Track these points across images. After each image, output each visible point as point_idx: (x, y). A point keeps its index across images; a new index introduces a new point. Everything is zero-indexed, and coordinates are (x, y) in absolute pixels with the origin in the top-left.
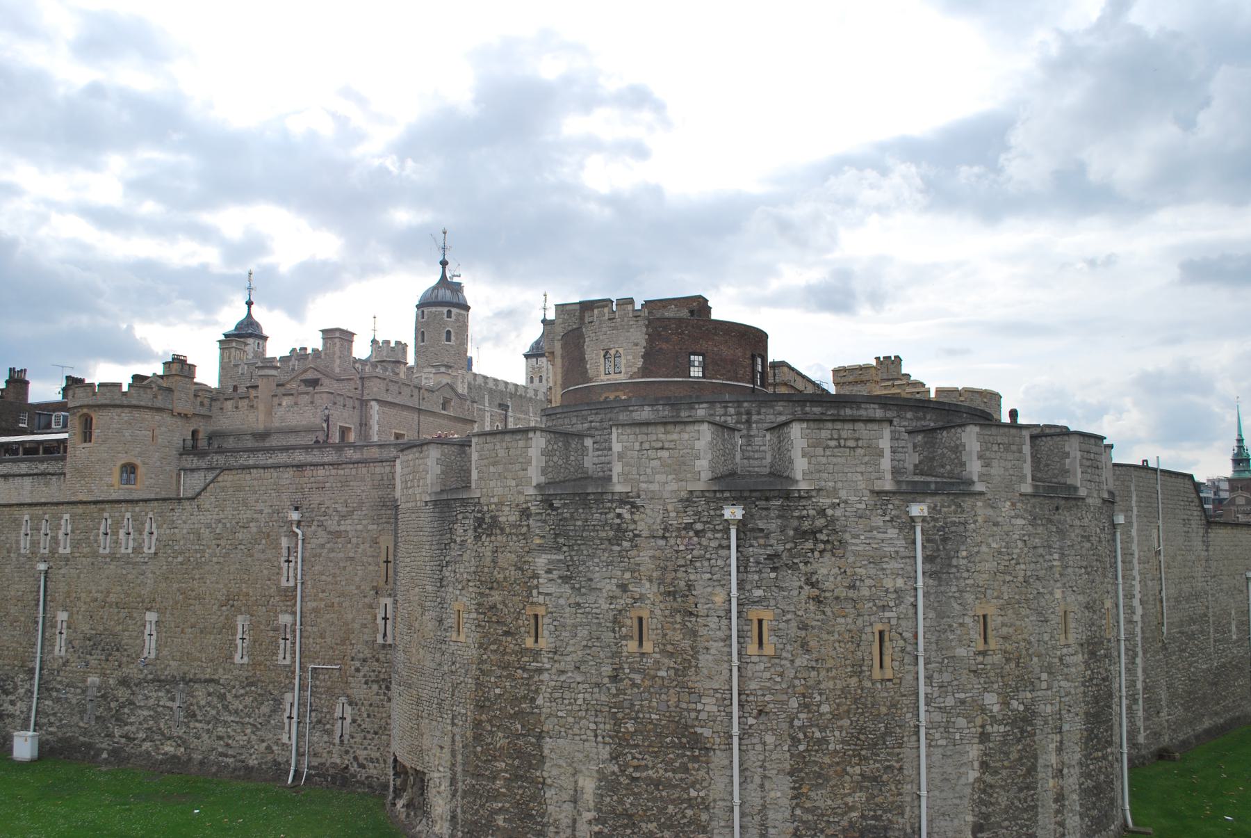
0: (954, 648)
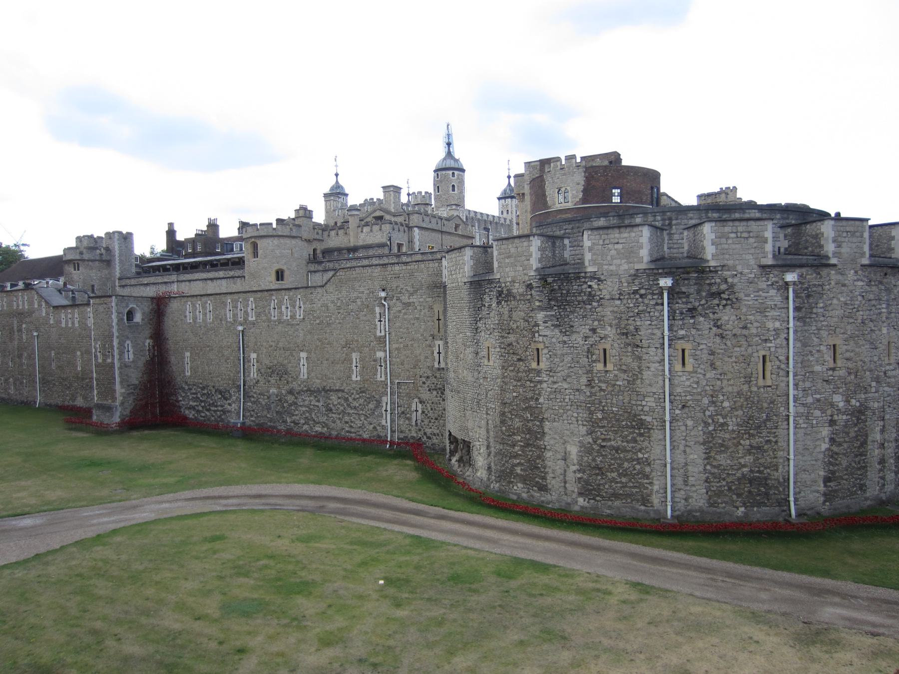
0: (813, 366)
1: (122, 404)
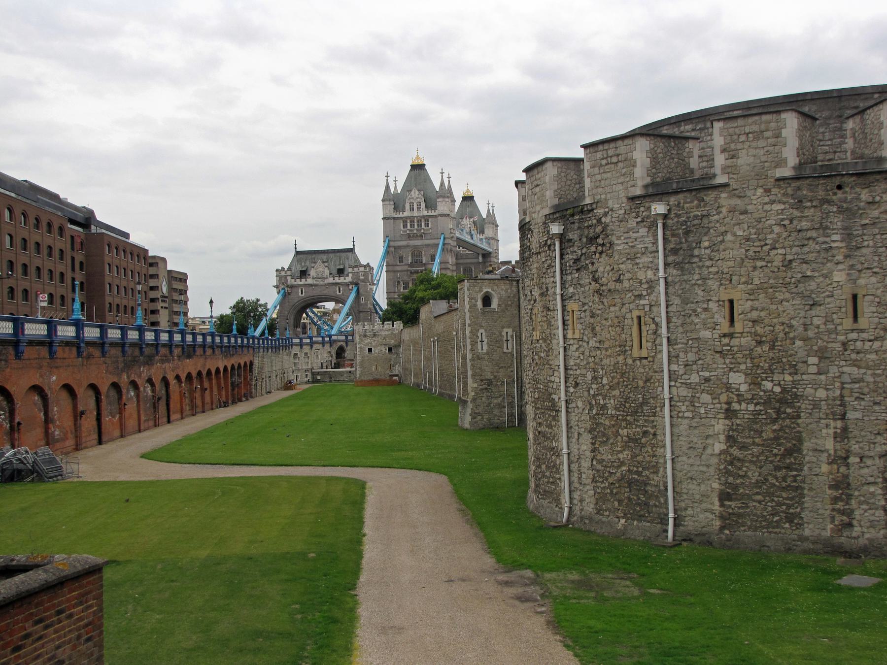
0: (698, 331)
1: (474, 400)
